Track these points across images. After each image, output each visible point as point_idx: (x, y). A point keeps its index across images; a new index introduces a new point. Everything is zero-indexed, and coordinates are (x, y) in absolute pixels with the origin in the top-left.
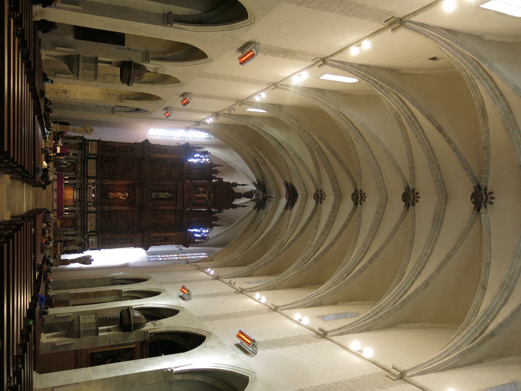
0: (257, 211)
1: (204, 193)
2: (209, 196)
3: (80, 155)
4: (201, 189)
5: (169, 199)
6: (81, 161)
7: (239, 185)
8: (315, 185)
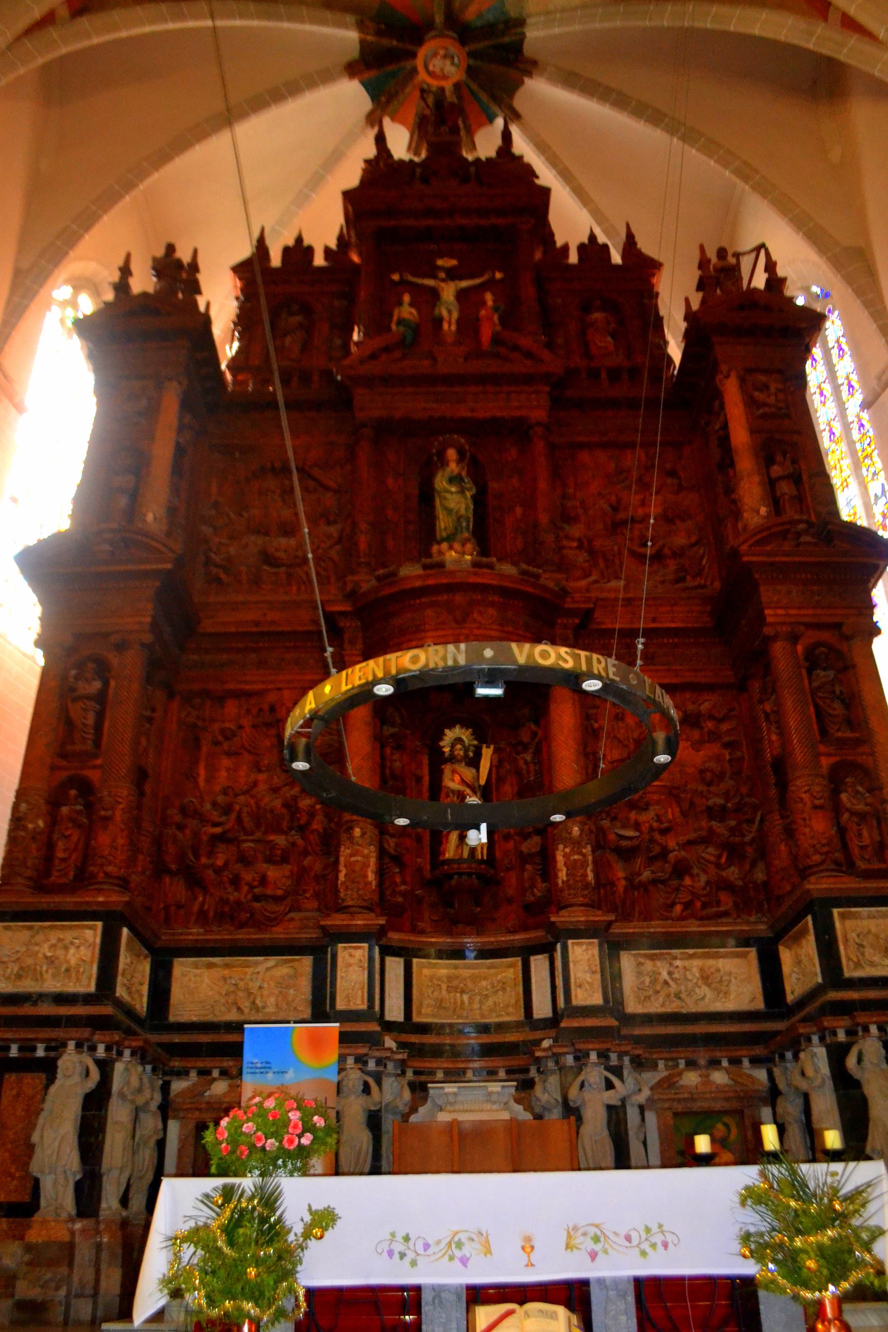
1: (434, 295)
2: (452, 275)
3: (100, 1063)
6: (183, 1073)
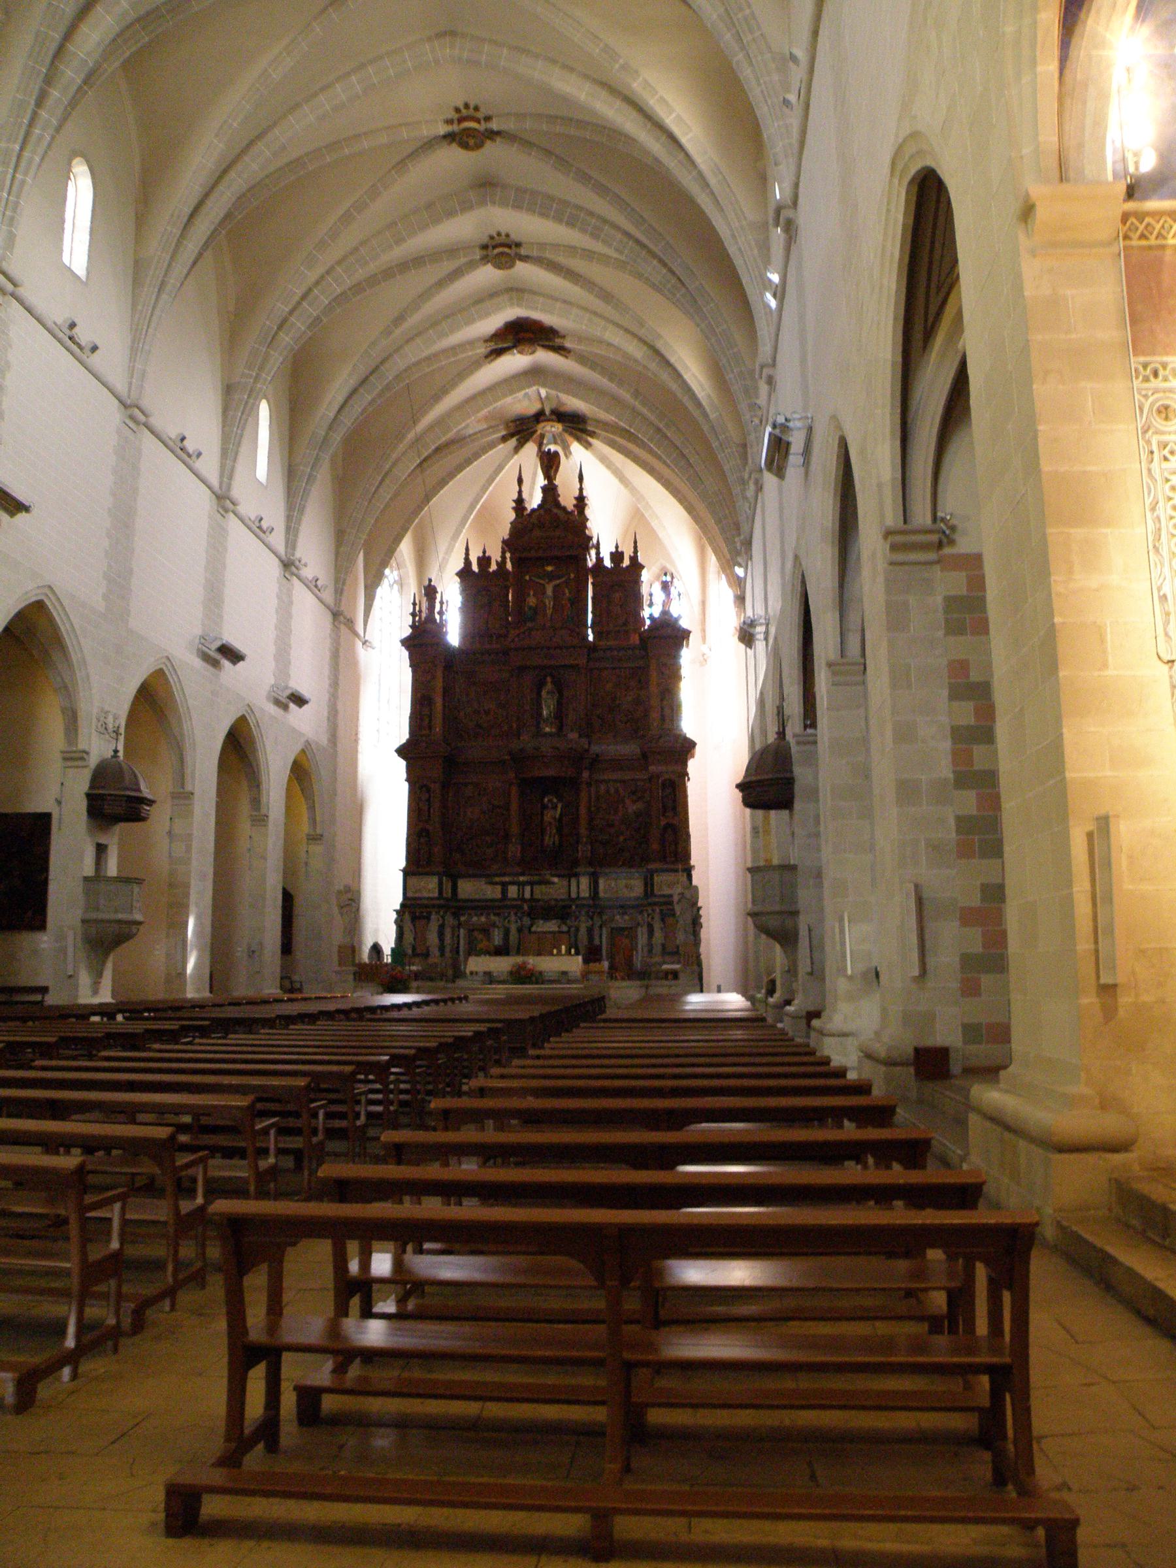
0: (592, 437)
1: (544, 593)
2: (551, 577)
3: (442, 917)
4: (532, 601)
5: (559, 687)
7: (520, 492)
8: (471, 265)
